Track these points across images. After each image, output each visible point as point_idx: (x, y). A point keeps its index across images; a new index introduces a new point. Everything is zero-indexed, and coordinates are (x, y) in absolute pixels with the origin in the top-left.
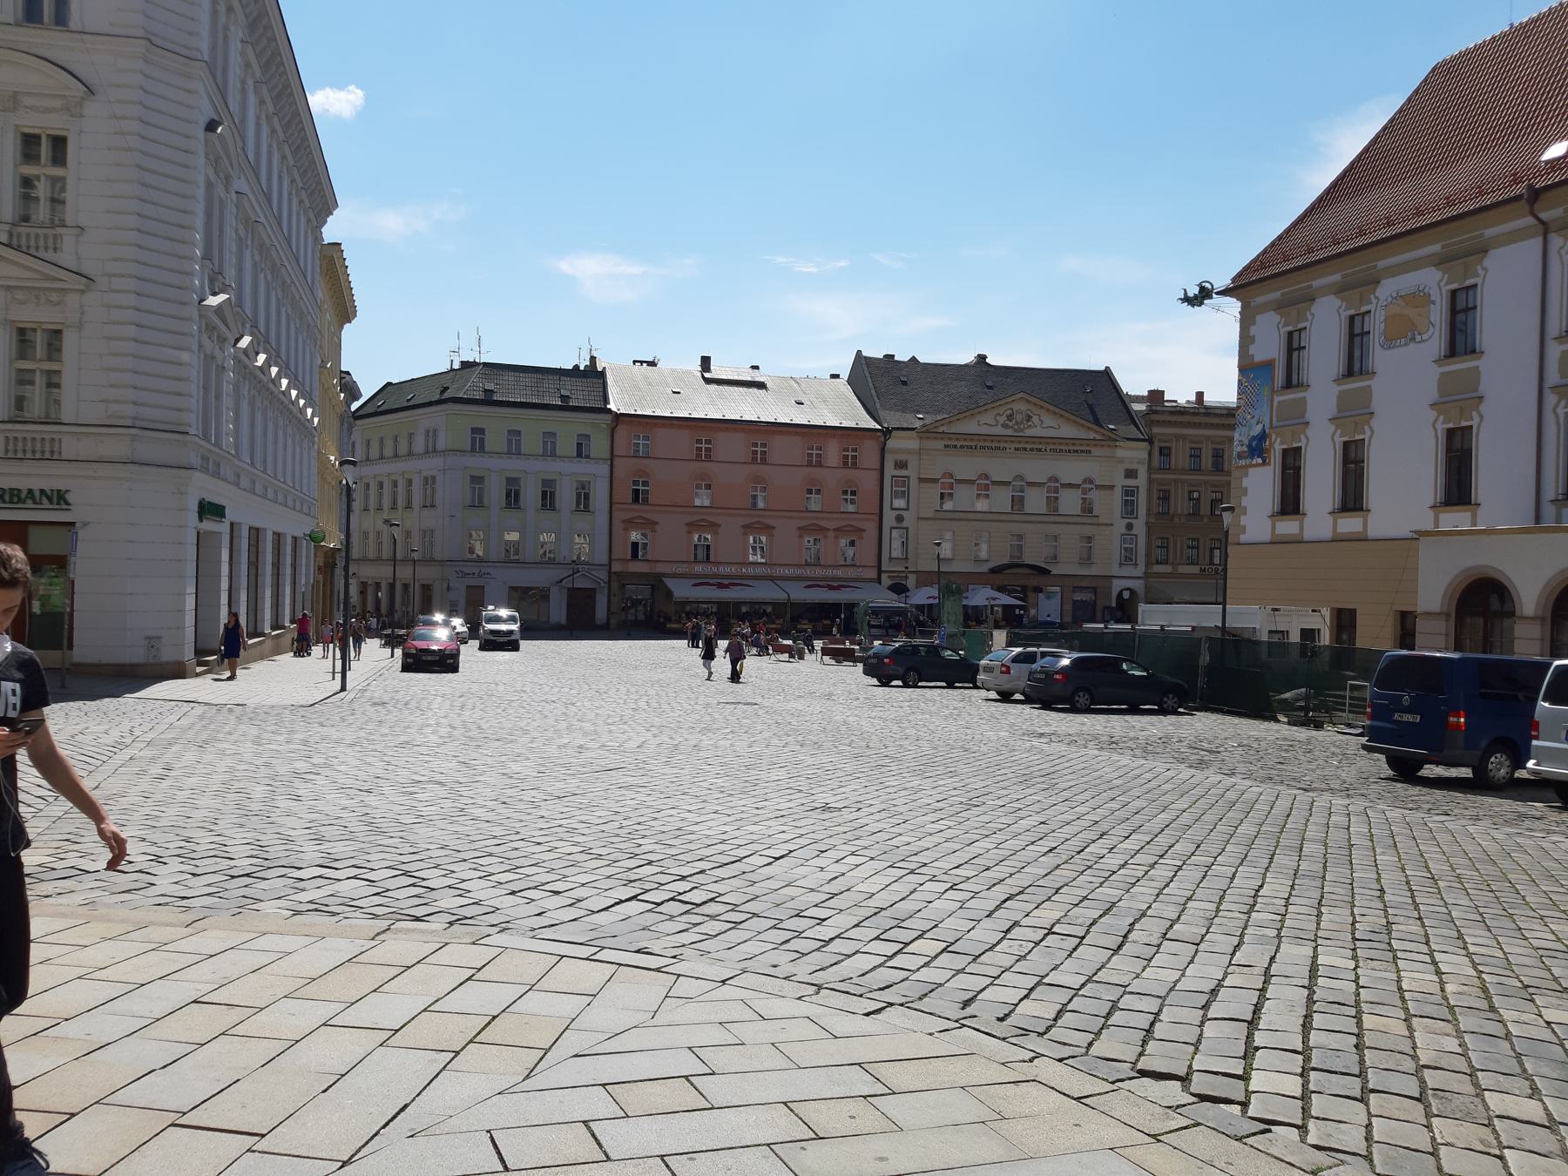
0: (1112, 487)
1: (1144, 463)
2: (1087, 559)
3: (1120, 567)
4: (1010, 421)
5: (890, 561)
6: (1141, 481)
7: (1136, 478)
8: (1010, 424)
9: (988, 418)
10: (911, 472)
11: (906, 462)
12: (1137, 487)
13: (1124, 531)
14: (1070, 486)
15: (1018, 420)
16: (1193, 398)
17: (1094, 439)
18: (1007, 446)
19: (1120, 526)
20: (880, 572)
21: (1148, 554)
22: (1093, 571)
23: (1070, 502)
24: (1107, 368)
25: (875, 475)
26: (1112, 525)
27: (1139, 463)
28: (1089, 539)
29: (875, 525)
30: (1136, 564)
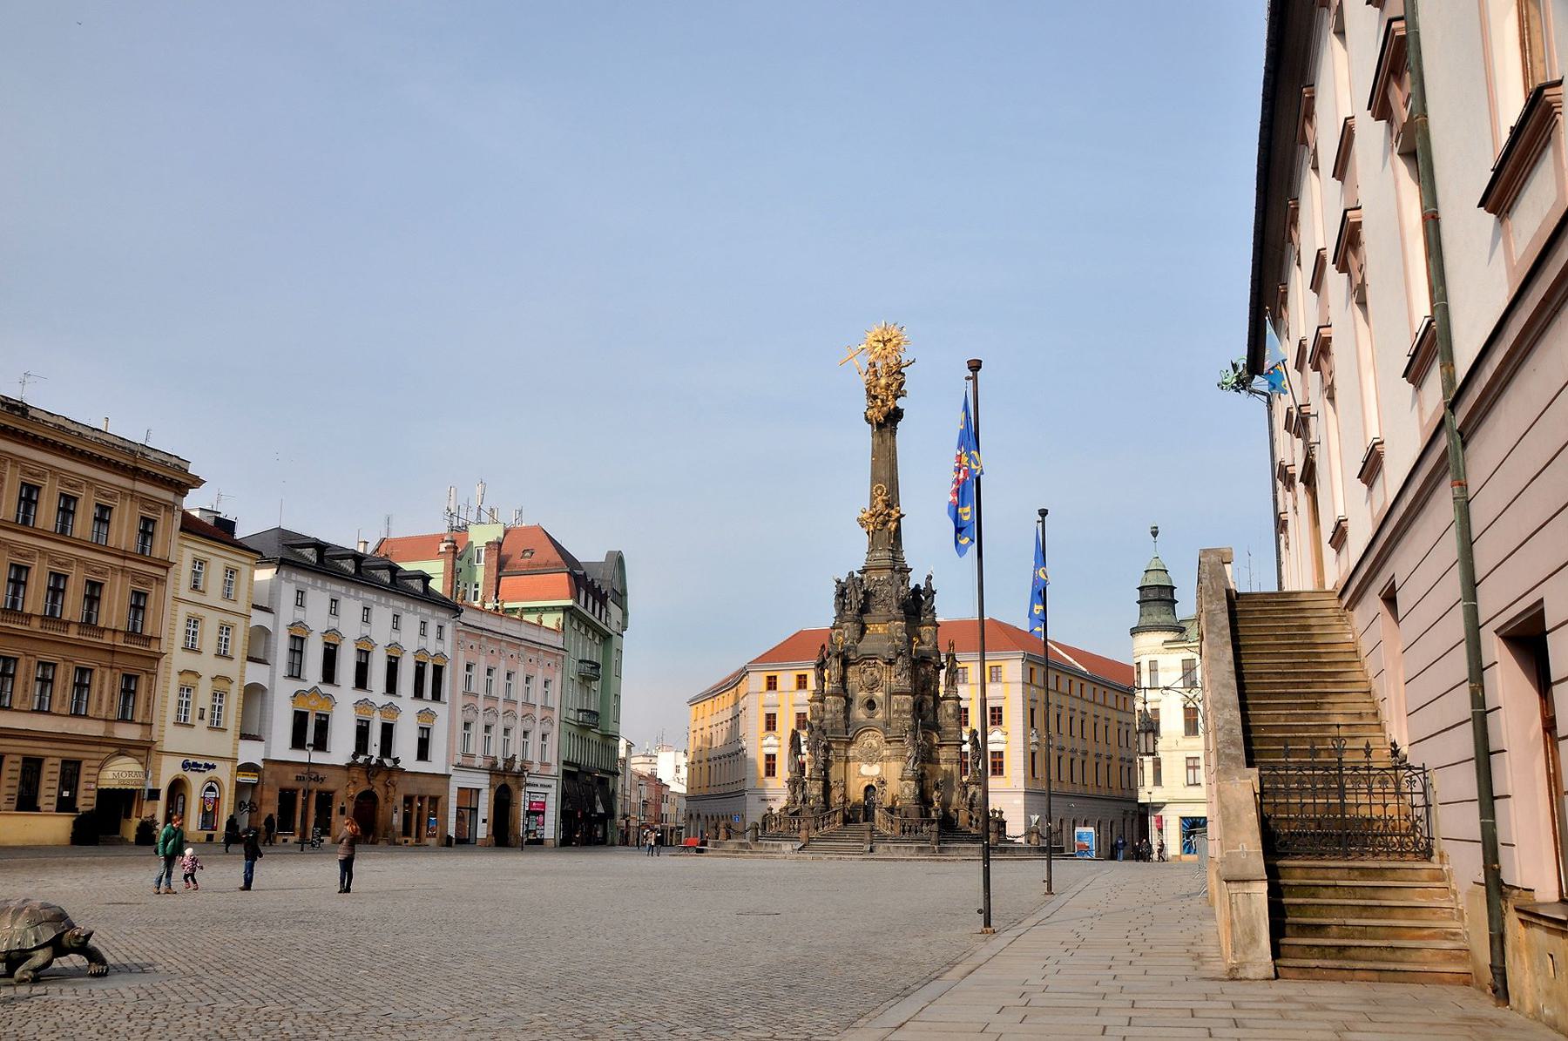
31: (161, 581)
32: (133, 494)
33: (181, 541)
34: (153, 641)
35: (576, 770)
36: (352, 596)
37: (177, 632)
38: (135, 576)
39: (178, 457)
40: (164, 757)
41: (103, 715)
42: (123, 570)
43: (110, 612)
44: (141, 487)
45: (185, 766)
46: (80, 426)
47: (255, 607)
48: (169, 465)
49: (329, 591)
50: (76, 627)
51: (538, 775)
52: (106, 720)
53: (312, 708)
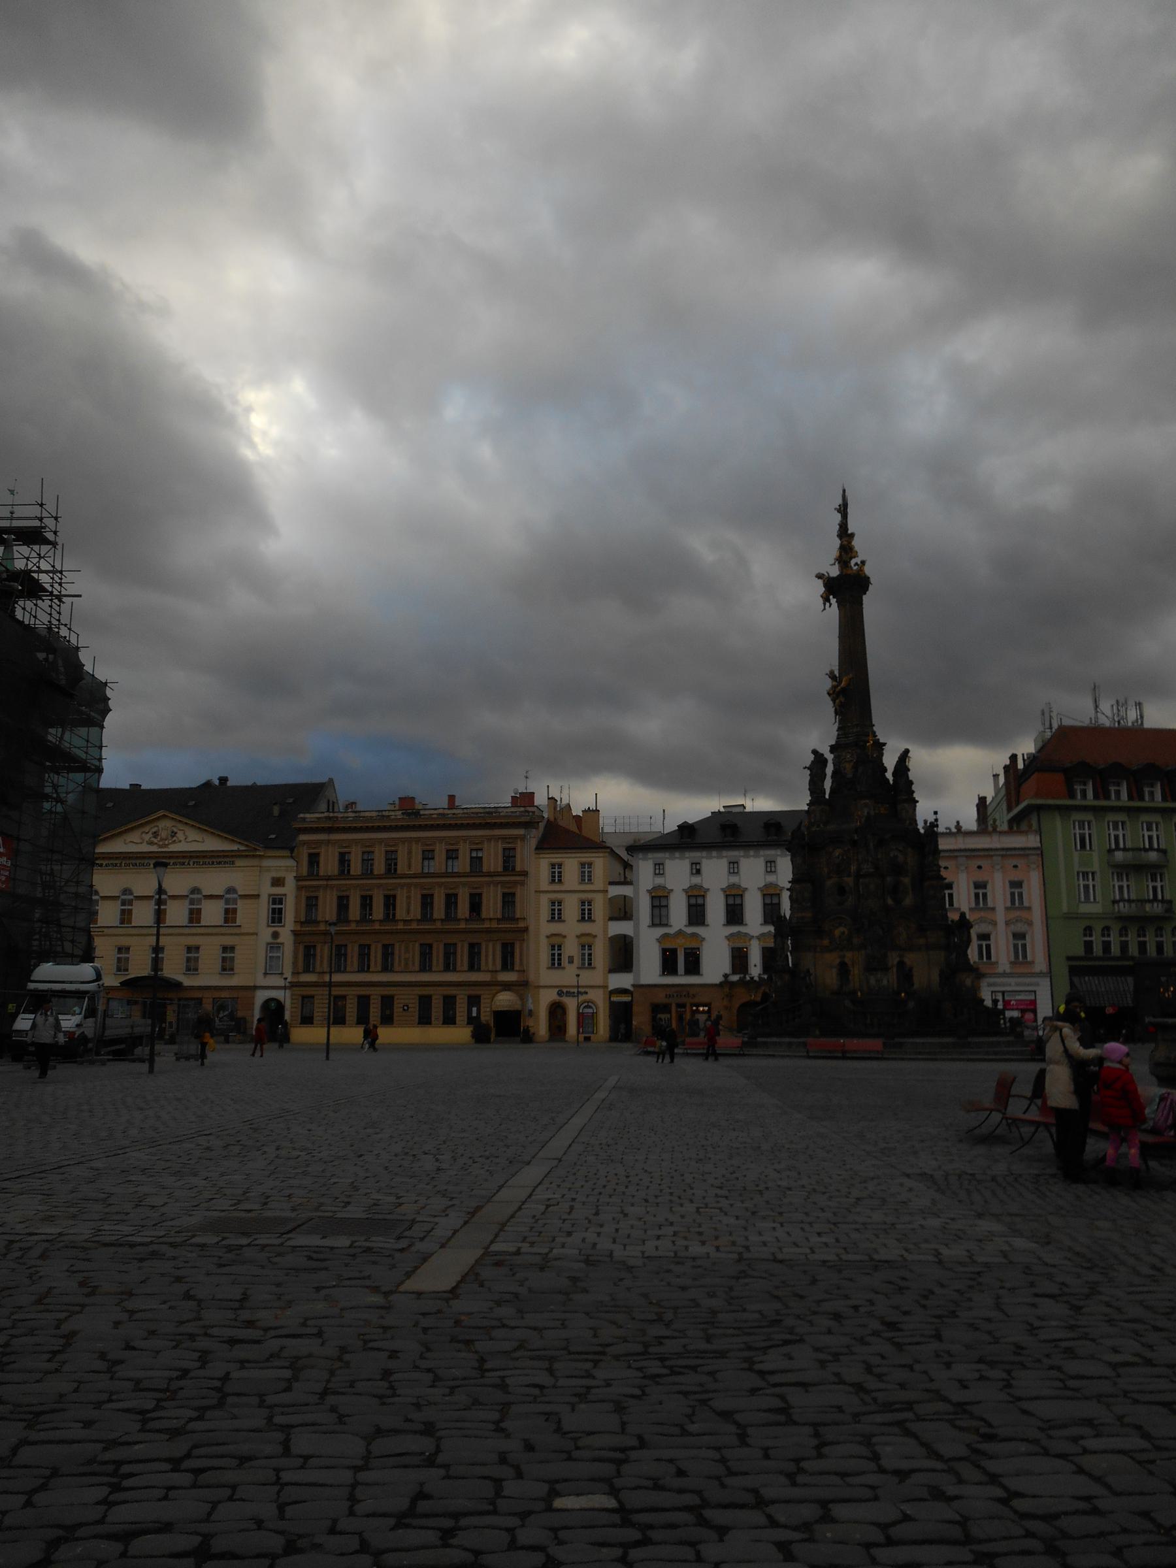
0: (257, 896)
2: (227, 967)
3: (265, 977)
4: (155, 837)
6: (289, 888)
7: (284, 886)
8: (155, 841)
9: (134, 836)
12: (285, 895)
13: (270, 940)
14: (211, 897)
16: (445, 803)
17: (239, 851)
19: (266, 934)
21: (295, 963)
22: (234, 981)
23: (212, 913)
24: (331, 780)
31: (522, 883)
33: (537, 856)
35: (1131, 963)
36: (715, 857)
40: (542, 991)
44: (497, 832)
45: (560, 994)
47: (611, 883)
49: (726, 857)
51: (1004, 975)
53: (680, 946)
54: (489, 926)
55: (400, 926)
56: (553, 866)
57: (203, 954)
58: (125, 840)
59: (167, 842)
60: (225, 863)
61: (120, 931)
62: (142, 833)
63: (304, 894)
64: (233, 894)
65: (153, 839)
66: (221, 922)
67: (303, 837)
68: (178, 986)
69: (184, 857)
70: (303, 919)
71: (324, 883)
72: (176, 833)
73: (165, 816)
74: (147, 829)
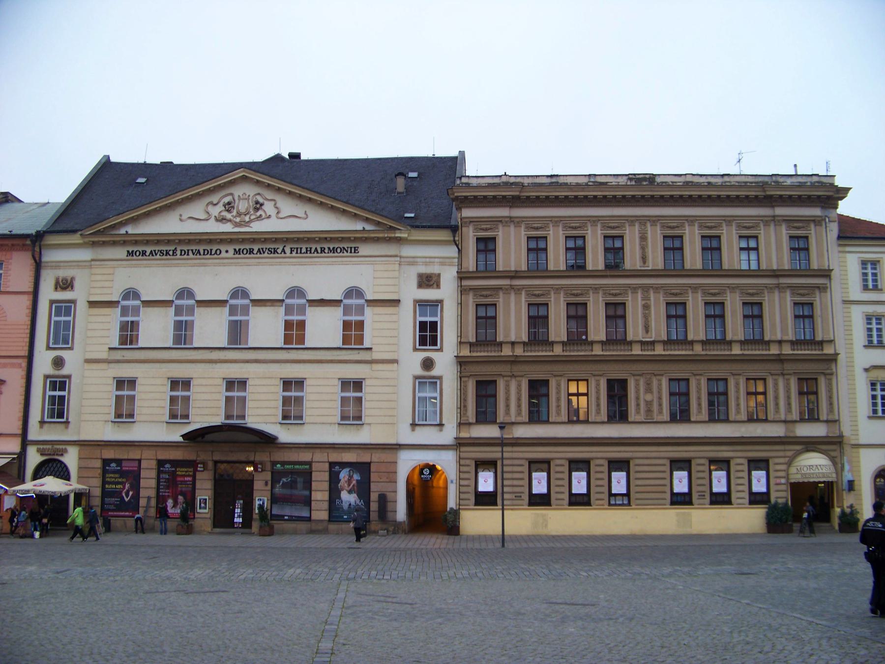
0: (396, 302)
1: (451, 265)
3: (413, 430)
4: (229, 211)
5: (41, 427)
7: (438, 287)
8: (228, 216)
9: (197, 209)
10: (79, 294)
11: (73, 279)
13: (420, 372)
14: (322, 302)
15: (242, 210)
18: (223, 248)
19: (412, 361)
20: (25, 443)
21: (462, 407)
25: (26, 301)
26: (395, 361)
27: (442, 264)
28: (358, 385)
29: (21, 373)
30: (441, 425)
31: (823, 289)
32: (775, 220)
33: (841, 249)
34: (825, 345)
37: (854, 332)
38: (793, 288)
39: (817, 175)
40: (863, 452)
41: (783, 417)
42: (778, 286)
43: (773, 325)
44: (780, 211)
46: (709, 177)
48: (809, 184)
50: (600, 345)
52: (785, 422)
54: (777, 352)
55: (637, 351)
56: (864, 263)
57: (310, 393)
58: (181, 215)
59: (247, 219)
60: (343, 250)
61: (175, 355)
62: (207, 205)
63: (471, 300)
64: (357, 298)
65: (225, 214)
66: (339, 344)
67: (467, 213)
68: (267, 440)
69: (276, 240)
70: (472, 339)
71: (506, 282)
72: (262, 205)
73: (244, 179)
74: (215, 198)
